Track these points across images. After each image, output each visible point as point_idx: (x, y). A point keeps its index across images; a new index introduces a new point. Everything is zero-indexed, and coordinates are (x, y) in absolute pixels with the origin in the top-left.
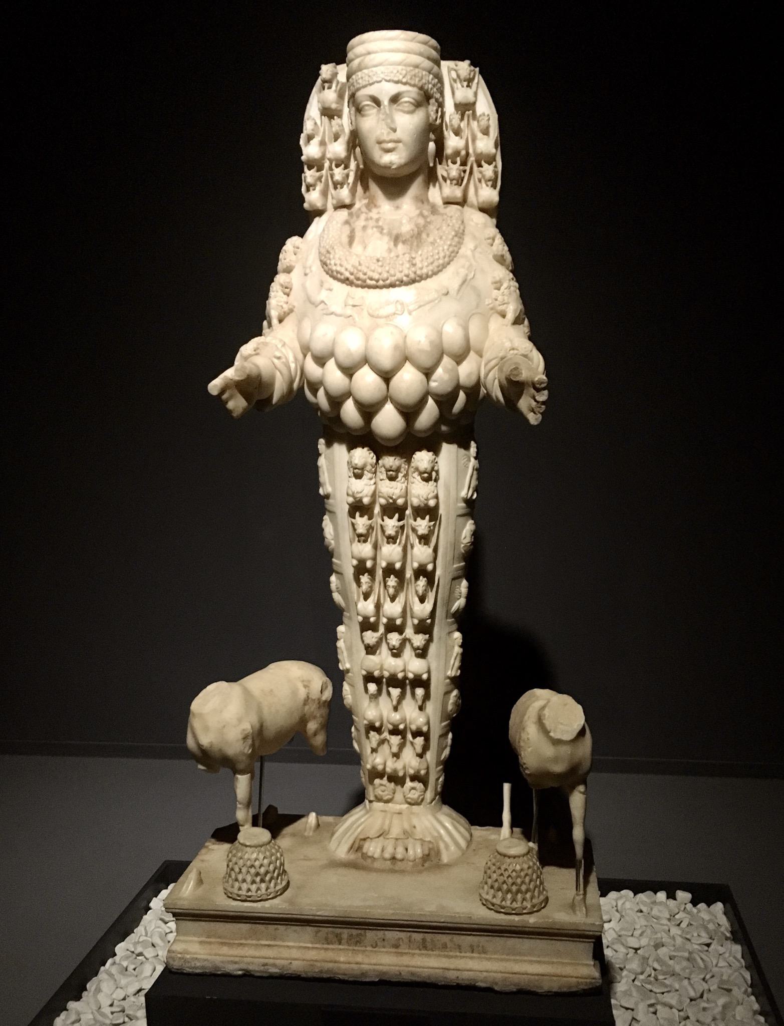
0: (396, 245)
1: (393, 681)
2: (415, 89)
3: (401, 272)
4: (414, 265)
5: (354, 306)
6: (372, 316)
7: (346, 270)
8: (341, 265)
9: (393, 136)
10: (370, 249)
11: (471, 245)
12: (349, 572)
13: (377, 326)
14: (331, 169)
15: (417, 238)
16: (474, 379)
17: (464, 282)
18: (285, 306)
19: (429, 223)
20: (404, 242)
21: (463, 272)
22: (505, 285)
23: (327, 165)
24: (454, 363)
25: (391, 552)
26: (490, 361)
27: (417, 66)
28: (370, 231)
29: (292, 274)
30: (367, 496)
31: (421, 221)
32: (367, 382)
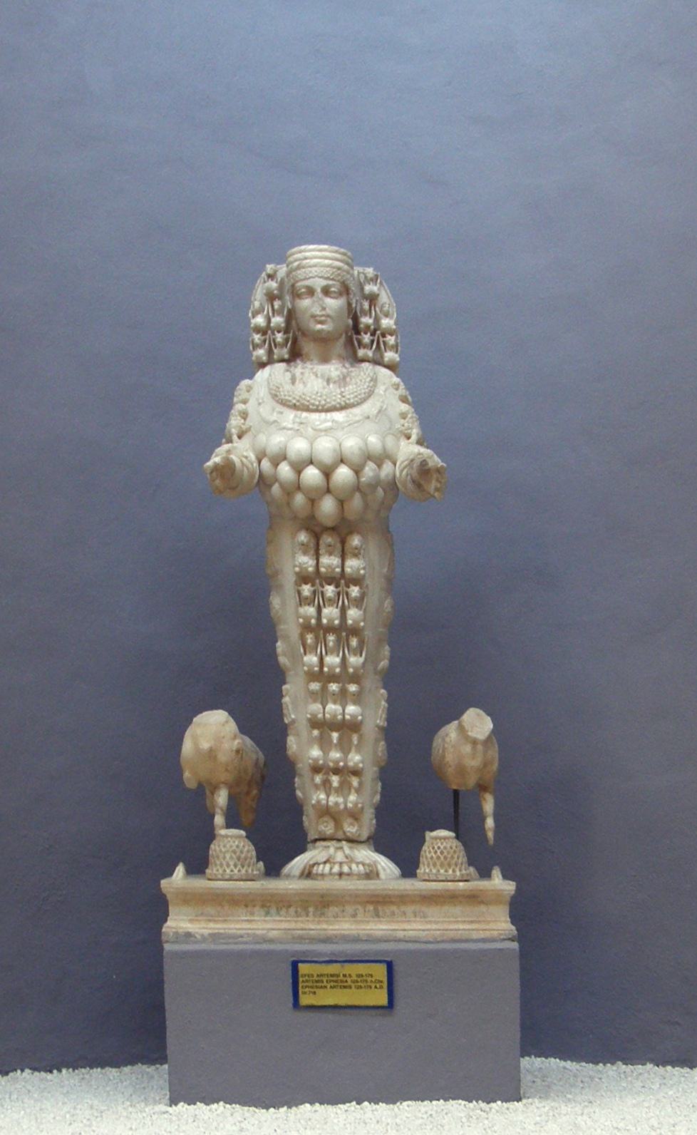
0: (328, 384)
2: (338, 283)
4: (344, 397)
5: (301, 423)
6: (315, 430)
7: (294, 398)
8: (290, 396)
9: (324, 313)
10: (309, 385)
13: (320, 436)
14: (274, 334)
15: (343, 380)
18: (243, 426)
20: (335, 382)
22: (409, 416)
23: (269, 332)
25: (331, 613)
27: (339, 269)
28: (307, 375)
29: (247, 405)
30: (311, 566)
31: (345, 370)
32: (312, 475)
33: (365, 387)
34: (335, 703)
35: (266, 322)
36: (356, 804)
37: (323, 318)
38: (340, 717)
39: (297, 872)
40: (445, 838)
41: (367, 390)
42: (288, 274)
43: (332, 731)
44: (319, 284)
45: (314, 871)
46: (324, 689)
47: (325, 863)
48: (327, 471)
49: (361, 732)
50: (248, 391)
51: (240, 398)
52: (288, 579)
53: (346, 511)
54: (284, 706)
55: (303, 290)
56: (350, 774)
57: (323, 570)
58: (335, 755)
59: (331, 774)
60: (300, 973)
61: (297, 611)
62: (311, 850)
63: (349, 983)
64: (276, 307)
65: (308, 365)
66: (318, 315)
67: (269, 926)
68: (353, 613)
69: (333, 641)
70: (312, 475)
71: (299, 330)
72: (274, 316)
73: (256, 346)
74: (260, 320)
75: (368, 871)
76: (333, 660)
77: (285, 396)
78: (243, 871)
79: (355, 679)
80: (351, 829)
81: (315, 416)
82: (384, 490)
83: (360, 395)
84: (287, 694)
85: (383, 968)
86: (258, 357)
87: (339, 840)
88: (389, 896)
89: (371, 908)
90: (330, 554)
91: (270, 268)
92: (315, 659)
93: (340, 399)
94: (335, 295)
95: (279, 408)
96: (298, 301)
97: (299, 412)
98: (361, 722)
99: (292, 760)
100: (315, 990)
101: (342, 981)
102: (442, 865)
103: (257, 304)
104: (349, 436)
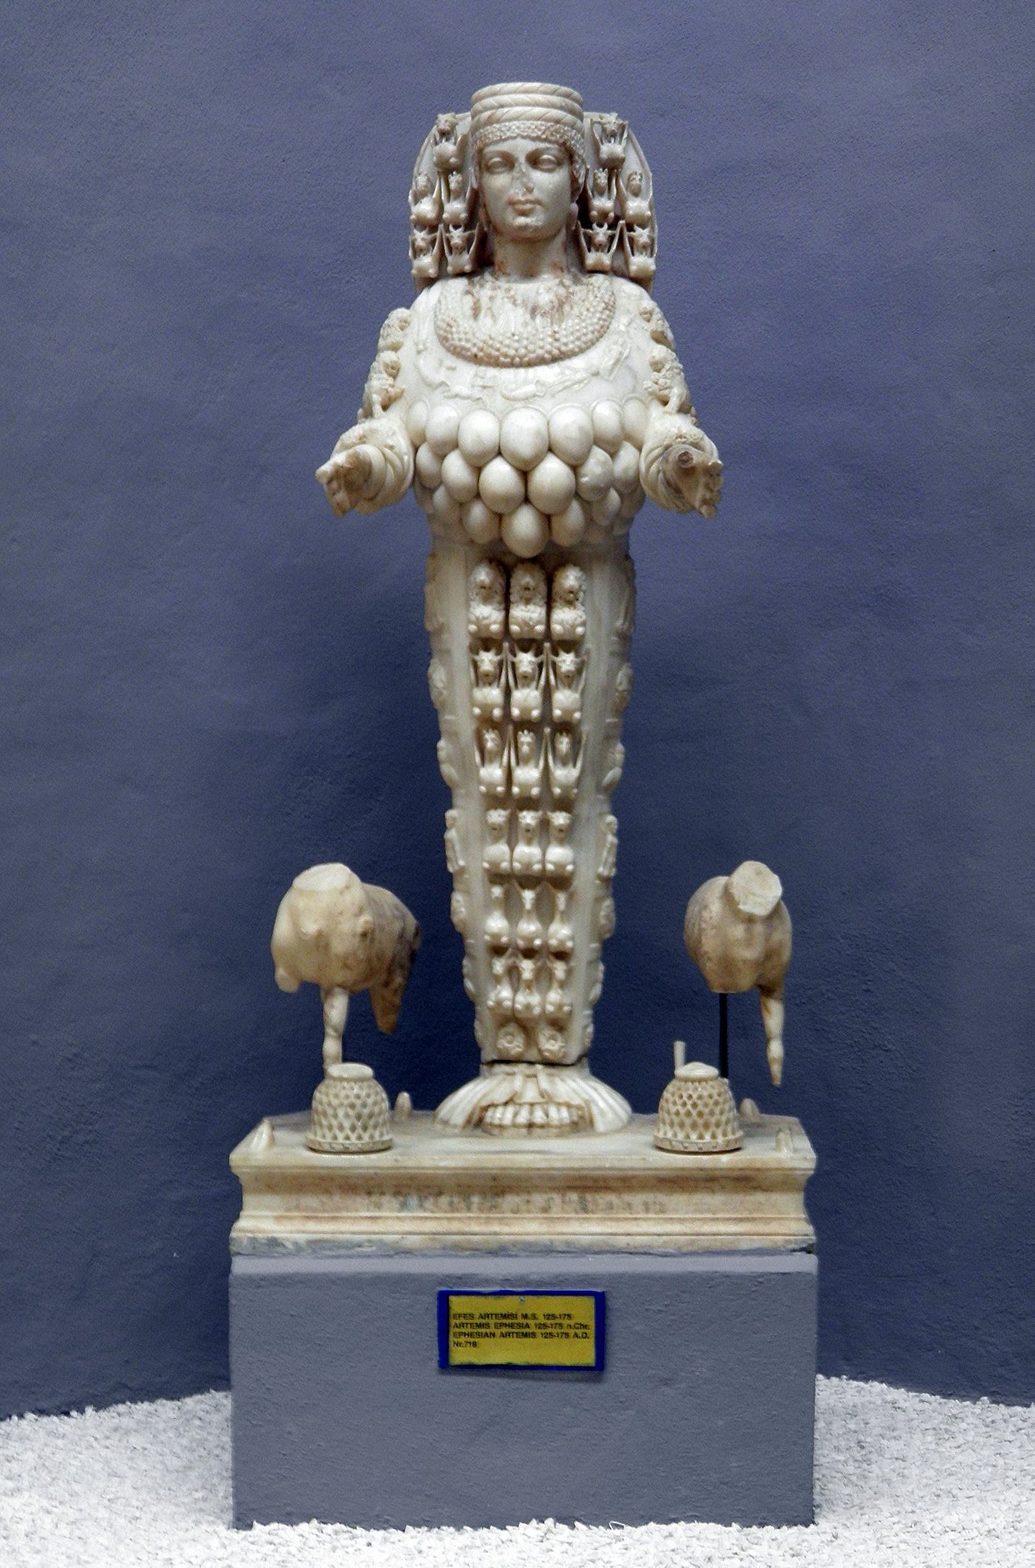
1: (528, 880)
3: (542, 348)
4: (557, 340)
5: (484, 387)
6: (508, 399)
7: (475, 345)
8: (468, 341)
9: (530, 197)
10: (501, 322)
11: (624, 320)
12: (467, 729)
14: (448, 231)
16: (631, 473)
17: (617, 362)
19: (573, 294)
20: (544, 315)
21: (616, 349)
23: (441, 226)
24: (607, 456)
25: (527, 698)
26: (651, 451)
27: (557, 121)
28: (498, 301)
31: (562, 291)
32: (500, 476)
33: (595, 320)
34: (529, 842)
35: (437, 208)
36: (560, 1007)
37: (528, 206)
38: (537, 867)
39: (459, 1118)
40: (700, 1080)
41: (597, 327)
42: (475, 128)
43: (524, 887)
44: (522, 148)
45: (488, 1119)
46: (513, 820)
47: (506, 1104)
48: (524, 469)
49: (571, 889)
50: (402, 329)
51: (390, 340)
52: (458, 640)
53: (554, 532)
54: (448, 845)
55: (497, 159)
56: (551, 957)
57: (514, 628)
58: (529, 927)
59: (520, 956)
60: (452, 1312)
61: (471, 696)
62: (486, 1078)
63: (532, 1329)
64: (453, 186)
65: (503, 283)
66: (520, 202)
67: (408, 1227)
68: (564, 698)
69: (529, 744)
70: (500, 476)
71: (489, 222)
72: (449, 200)
73: (418, 252)
74: (426, 208)
75: (575, 1118)
76: (528, 775)
77: (460, 340)
78: (366, 1137)
79: (564, 804)
80: (550, 1045)
81: (508, 375)
82: (620, 494)
83: (585, 335)
84: (453, 825)
85: (589, 1303)
86: (420, 270)
87: (531, 1063)
88: (605, 1179)
89: (574, 1196)
90: (528, 601)
91: (444, 120)
93: (551, 344)
94: (550, 167)
95: (450, 360)
96: (486, 176)
97: (483, 368)
98: (573, 873)
99: (458, 929)
100: (476, 1340)
101: (520, 1326)
102: (694, 1126)
103: (421, 181)
104: (564, 408)
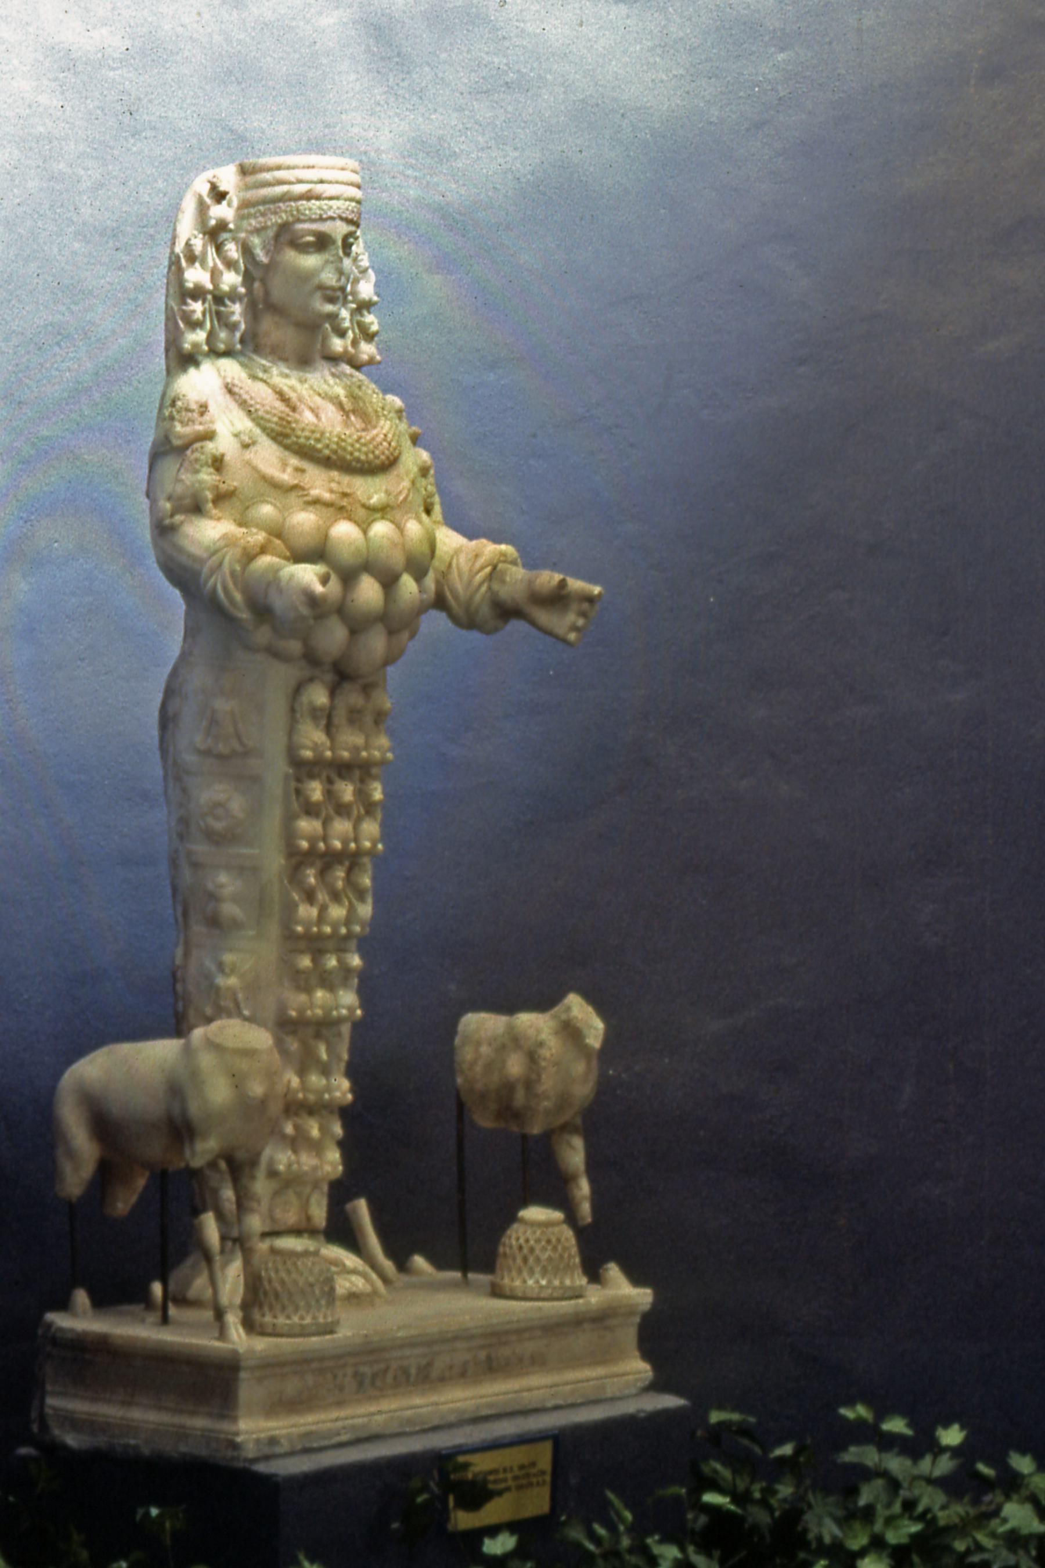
13: (374, 520)
55: (311, 239)
92: (314, 912)
95: (294, 461)
